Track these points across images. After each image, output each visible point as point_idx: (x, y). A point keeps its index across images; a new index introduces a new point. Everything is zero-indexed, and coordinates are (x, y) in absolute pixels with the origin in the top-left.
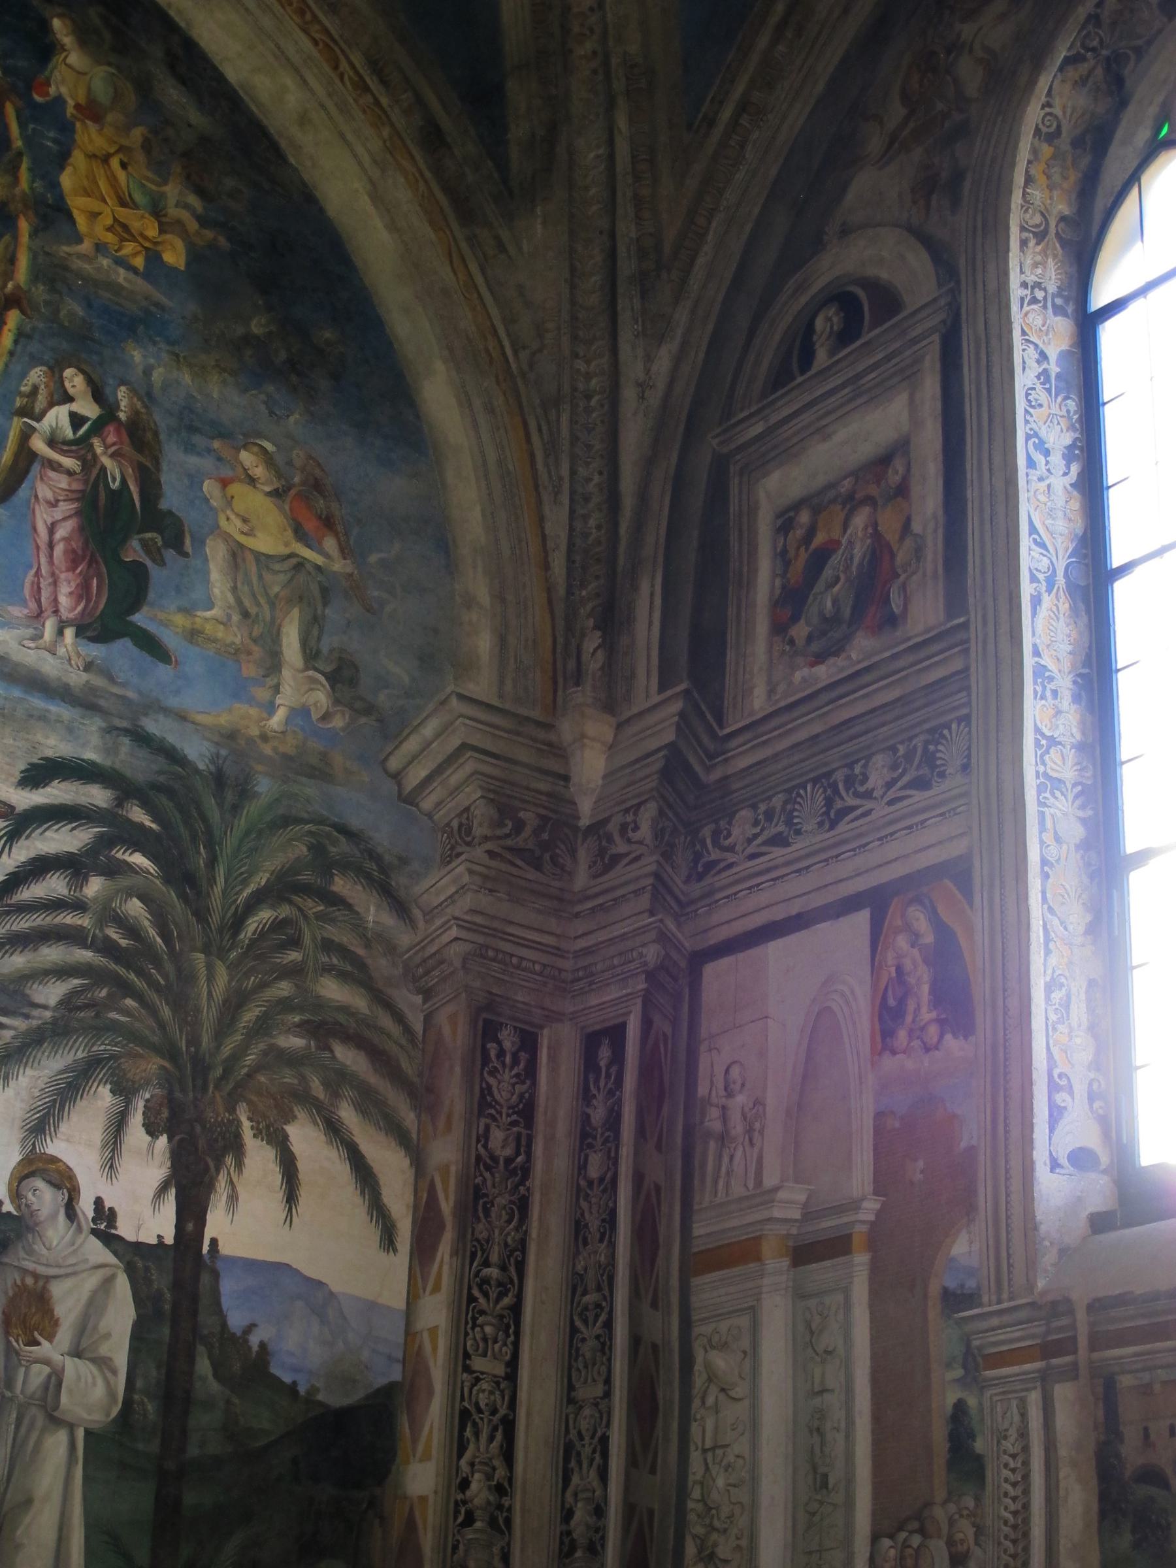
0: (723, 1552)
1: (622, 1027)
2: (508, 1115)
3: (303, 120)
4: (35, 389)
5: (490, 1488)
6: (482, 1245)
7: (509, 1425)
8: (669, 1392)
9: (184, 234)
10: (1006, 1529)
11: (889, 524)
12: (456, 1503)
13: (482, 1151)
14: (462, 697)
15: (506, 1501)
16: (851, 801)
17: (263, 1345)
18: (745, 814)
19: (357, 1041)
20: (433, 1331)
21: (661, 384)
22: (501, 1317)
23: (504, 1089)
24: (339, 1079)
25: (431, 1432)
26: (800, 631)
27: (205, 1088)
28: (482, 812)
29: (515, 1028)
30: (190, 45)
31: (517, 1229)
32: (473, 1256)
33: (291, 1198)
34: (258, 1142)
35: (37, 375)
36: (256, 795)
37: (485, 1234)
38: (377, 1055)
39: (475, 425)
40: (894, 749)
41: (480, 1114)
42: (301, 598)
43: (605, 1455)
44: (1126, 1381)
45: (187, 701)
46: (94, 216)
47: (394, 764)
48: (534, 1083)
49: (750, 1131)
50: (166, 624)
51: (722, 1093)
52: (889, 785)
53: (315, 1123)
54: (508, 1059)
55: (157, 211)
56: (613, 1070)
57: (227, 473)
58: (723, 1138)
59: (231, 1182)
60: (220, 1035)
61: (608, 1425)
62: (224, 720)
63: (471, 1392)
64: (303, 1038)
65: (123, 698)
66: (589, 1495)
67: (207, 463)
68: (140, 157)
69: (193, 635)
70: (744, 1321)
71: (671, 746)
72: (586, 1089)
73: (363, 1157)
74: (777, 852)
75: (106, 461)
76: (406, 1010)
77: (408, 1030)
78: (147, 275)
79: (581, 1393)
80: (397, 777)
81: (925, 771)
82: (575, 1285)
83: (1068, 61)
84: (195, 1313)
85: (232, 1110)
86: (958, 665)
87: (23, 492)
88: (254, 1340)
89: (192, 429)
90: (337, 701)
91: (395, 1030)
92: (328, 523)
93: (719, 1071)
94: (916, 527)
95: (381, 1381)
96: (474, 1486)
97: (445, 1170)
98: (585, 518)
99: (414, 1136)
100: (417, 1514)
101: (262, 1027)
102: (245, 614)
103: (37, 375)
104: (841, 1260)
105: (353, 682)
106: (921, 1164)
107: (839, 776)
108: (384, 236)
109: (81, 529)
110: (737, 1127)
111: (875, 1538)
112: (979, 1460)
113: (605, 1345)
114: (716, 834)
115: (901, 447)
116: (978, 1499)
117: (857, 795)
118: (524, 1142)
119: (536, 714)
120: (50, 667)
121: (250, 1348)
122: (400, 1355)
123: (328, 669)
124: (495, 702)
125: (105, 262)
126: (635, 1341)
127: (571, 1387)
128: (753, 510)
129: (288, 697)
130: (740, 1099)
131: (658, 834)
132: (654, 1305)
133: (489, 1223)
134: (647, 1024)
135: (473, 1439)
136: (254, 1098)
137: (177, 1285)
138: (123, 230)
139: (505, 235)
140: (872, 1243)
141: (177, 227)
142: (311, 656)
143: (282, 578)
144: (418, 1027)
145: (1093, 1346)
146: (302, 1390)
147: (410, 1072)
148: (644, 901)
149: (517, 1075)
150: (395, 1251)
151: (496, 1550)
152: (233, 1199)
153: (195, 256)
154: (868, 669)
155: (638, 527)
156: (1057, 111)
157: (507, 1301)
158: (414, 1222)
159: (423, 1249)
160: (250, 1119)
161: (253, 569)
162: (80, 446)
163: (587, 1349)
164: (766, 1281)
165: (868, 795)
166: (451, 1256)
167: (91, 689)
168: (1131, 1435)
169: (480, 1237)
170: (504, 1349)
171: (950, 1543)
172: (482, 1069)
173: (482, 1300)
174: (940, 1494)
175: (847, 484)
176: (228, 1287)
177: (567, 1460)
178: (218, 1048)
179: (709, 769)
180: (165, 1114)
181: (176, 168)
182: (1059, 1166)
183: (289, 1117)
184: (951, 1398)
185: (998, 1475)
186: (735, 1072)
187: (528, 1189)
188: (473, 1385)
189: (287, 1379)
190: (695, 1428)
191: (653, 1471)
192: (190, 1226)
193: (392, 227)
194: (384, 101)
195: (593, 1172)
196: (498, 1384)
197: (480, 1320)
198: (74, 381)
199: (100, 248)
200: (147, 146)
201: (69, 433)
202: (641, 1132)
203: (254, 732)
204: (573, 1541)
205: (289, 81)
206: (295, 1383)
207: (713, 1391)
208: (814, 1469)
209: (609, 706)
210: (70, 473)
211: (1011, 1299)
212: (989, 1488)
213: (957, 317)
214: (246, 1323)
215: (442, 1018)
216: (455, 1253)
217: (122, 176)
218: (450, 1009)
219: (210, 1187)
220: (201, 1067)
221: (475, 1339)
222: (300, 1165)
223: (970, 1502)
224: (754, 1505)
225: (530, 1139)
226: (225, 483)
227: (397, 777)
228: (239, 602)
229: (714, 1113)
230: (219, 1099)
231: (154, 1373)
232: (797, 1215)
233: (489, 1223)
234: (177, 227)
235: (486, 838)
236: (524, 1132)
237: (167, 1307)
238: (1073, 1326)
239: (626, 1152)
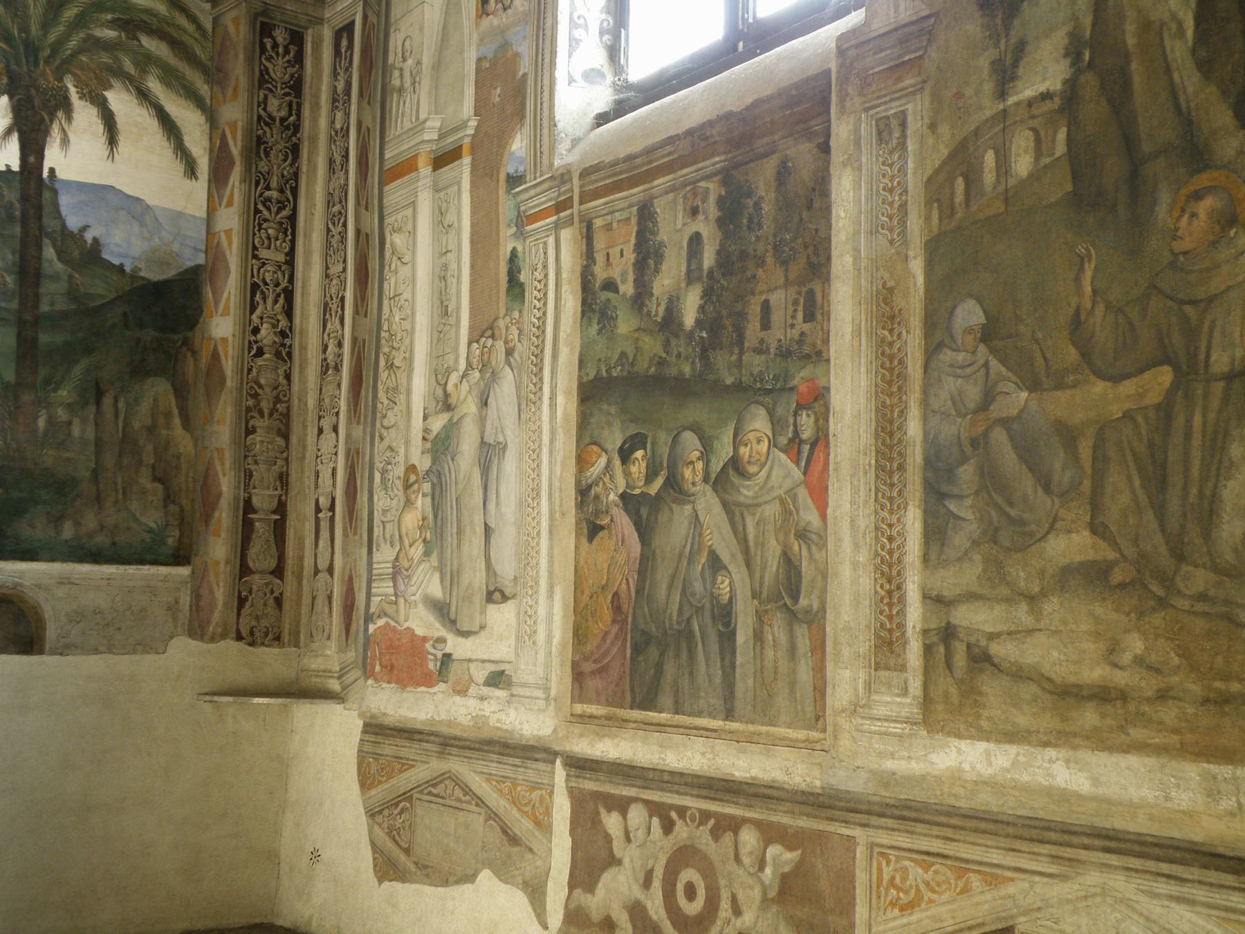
0: (397, 363)
1: (353, 22)
2: (282, 89)
5: (275, 333)
6: (264, 176)
7: (289, 295)
8: (373, 265)
10: (535, 330)
12: (250, 342)
13: (262, 113)
15: (288, 342)
17: (95, 240)
19: (159, 34)
20: (228, 232)
22: (281, 224)
23: (278, 70)
24: (145, 61)
25: (229, 298)
27: (36, 63)
29: (286, 28)
31: (291, 165)
32: (257, 183)
33: (112, 140)
34: (83, 103)
37: (266, 169)
38: (174, 43)
41: (260, 87)
43: (343, 309)
44: (598, 223)
48: (302, 67)
49: (414, 83)
51: (401, 59)
53: (128, 90)
54: (281, 50)
56: (348, 54)
58: (401, 90)
59: (63, 130)
60: (46, 26)
61: (344, 290)
63: (259, 272)
64: (115, 30)
66: (335, 334)
70: (409, 212)
72: (335, 69)
73: (168, 114)
76: (198, 14)
77: (200, 27)
79: (331, 272)
82: (329, 203)
84: (40, 218)
85: (60, 80)
88: (89, 236)
91: (190, 27)
93: (400, 44)
95: (189, 264)
96: (263, 332)
97: (233, 125)
99: (208, 101)
100: (220, 349)
101: (81, 21)
104: (456, 163)
106: (498, 90)
110: (408, 83)
111: (470, 344)
112: (522, 285)
113: (343, 240)
116: (520, 312)
118: (294, 107)
121: (85, 241)
122: (203, 248)
126: (358, 232)
127: (327, 268)
130: (410, 62)
132: (367, 209)
133: (269, 161)
134: (365, 17)
135: (261, 302)
136: (78, 72)
137: (24, 198)
140: (473, 150)
144: (209, 26)
145: (581, 203)
146: (128, 269)
147: (203, 57)
149: (288, 61)
150: (196, 178)
151: (281, 372)
152: (65, 141)
157: (285, 213)
158: (210, 160)
159: (218, 176)
160: (76, 87)
163: (334, 242)
164: (420, 184)
166: (240, 183)
168: (600, 258)
169: (262, 170)
170: (284, 244)
171: (506, 342)
172: (261, 57)
173: (265, 212)
174: (502, 312)
176: (65, 201)
177: (325, 315)
178: (45, 35)
180: (5, 80)
182: (574, 81)
183: (109, 87)
184: (509, 249)
185: (531, 294)
186: (408, 43)
187: (299, 139)
188: (260, 268)
189: (116, 262)
190: (386, 285)
191: (366, 316)
192: (32, 159)
195: (338, 126)
196: (280, 267)
197: (265, 225)
202: (361, 94)
204: (328, 364)
206: (122, 265)
207: (395, 259)
208: (442, 303)
211: (541, 176)
212: (526, 304)
214: (80, 225)
215: (228, 20)
216: (243, 181)
218: (234, 13)
219: (46, 132)
220: (32, 49)
221: (261, 238)
222: (117, 119)
223: (516, 314)
224: (413, 328)
225: (299, 105)
229: (396, 73)
230: (48, 71)
231: (10, 256)
232: (435, 137)
233: (269, 161)
236: (295, 100)
237: (18, 213)
238: (571, 190)
239: (354, 108)
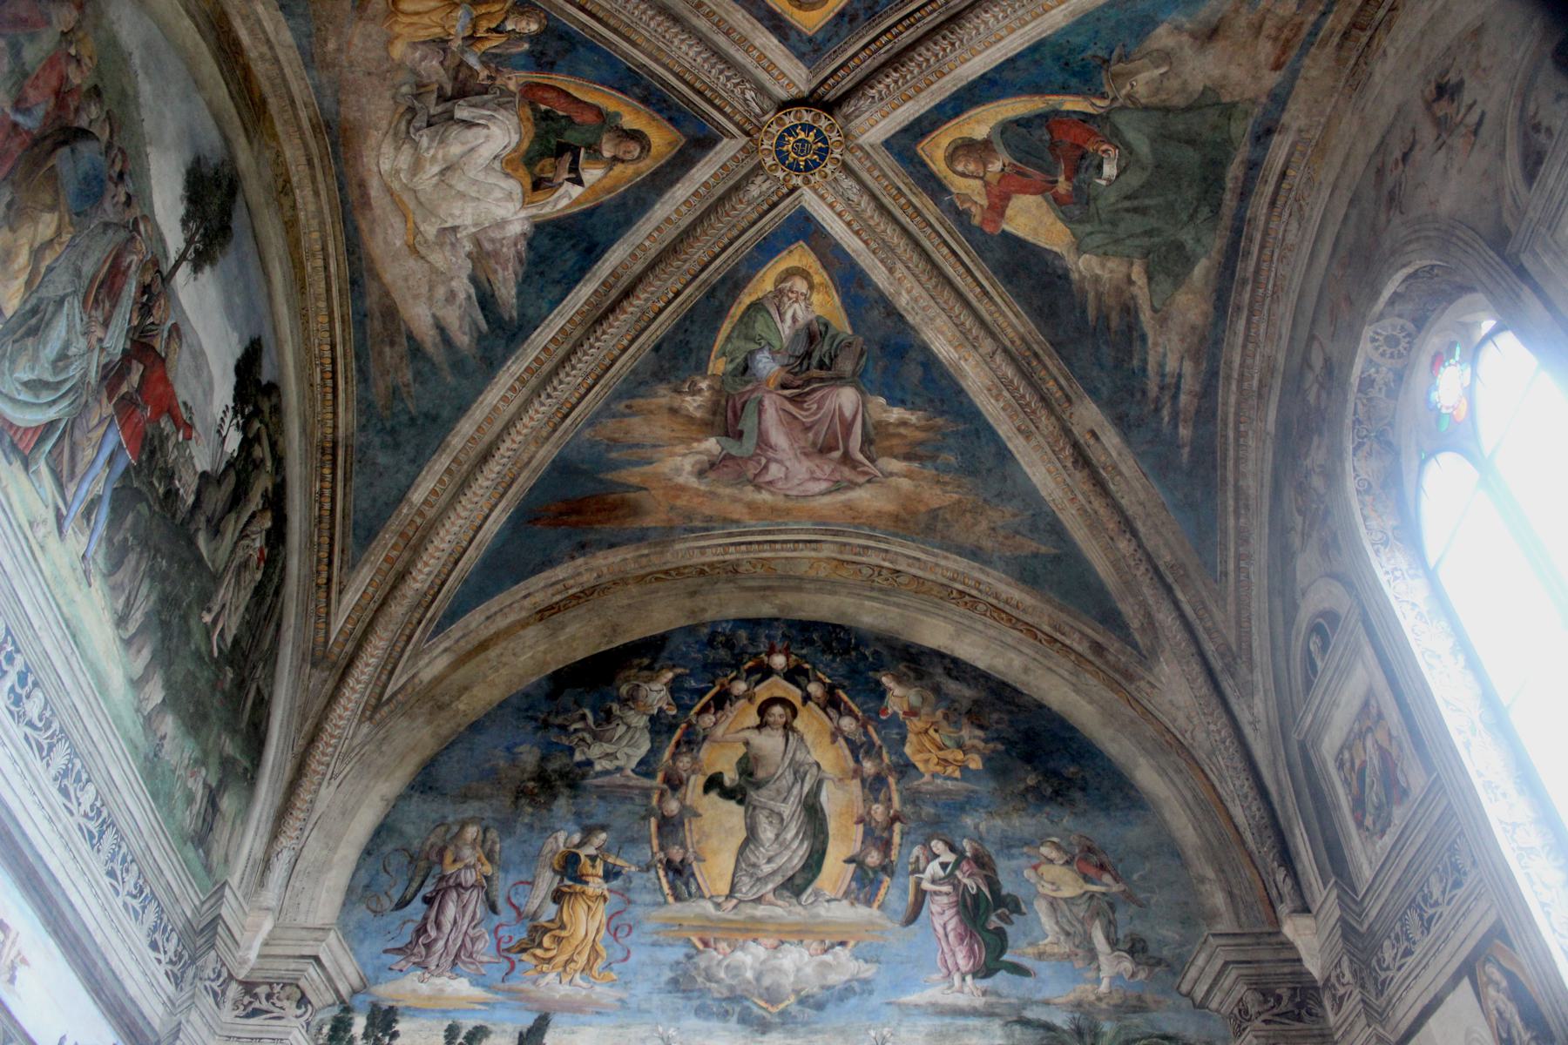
3: (1026, 670)
4: (918, 858)
9: (978, 751)
11: (1381, 735)
14: (1214, 935)
16: (1431, 911)
18: (1387, 943)
21: (1262, 717)
26: (1368, 821)
28: (1252, 1000)
30: (955, 661)
35: (917, 851)
36: (1104, 1034)
39: (1174, 784)
40: (1437, 869)
42: (1097, 914)
45: (1046, 993)
46: (927, 761)
47: (1185, 988)
50: (1024, 955)
52: (1444, 892)
55: (960, 746)
57: (1035, 861)
62: (1072, 997)
65: (1009, 1004)
67: (1023, 861)
68: (944, 723)
69: (1040, 956)
71: (1341, 919)
74: (1410, 960)
75: (966, 881)
78: (964, 779)
80: (1189, 995)
81: (1456, 875)
83: (1355, 450)
86: (1445, 802)
87: (924, 912)
89: (1009, 847)
90: (1138, 964)
92: (1102, 867)
94: (1394, 733)
98: (1249, 807)
102: (1068, 934)
103: (917, 851)
105: (1144, 950)
107: (1419, 899)
108: (1089, 708)
109: (961, 921)
114: (1378, 961)
115: (1370, 693)
117: (1432, 906)
119: (1267, 929)
120: (962, 1000)
123: (1127, 946)
124: (1238, 931)
125: (939, 781)
128: (1324, 763)
129: (1107, 972)
131: (1354, 974)
138: (945, 762)
139: (1152, 679)
141: (974, 748)
142: (1113, 943)
143: (1084, 907)
148: (1363, 1020)
153: (987, 760)
154: (1406, 826)
155: (1282, 799)
156: (1364, 476)
161: (1065, 907)
162: (950, 878)
165: (1436, 904)
167: (991, 1005)
175: (1356, 726)
179: (1361, 924)
181: (965, 720)
193: (1091, 701)
194: (1068, 642)
198: (938, 846)
199: (934, 775)
200: (946, 717)
201: (942, 874)
203: (1092, 998)
205: (1012, 655)
209: (1305, 909)
210: (947, 894)
213: (1363, 607)
217: (936, 736)
226: (1035, 868)
227: (1189, 995)
228: (1062, 929)
234: (974, 748)
235: (1259, 1013)
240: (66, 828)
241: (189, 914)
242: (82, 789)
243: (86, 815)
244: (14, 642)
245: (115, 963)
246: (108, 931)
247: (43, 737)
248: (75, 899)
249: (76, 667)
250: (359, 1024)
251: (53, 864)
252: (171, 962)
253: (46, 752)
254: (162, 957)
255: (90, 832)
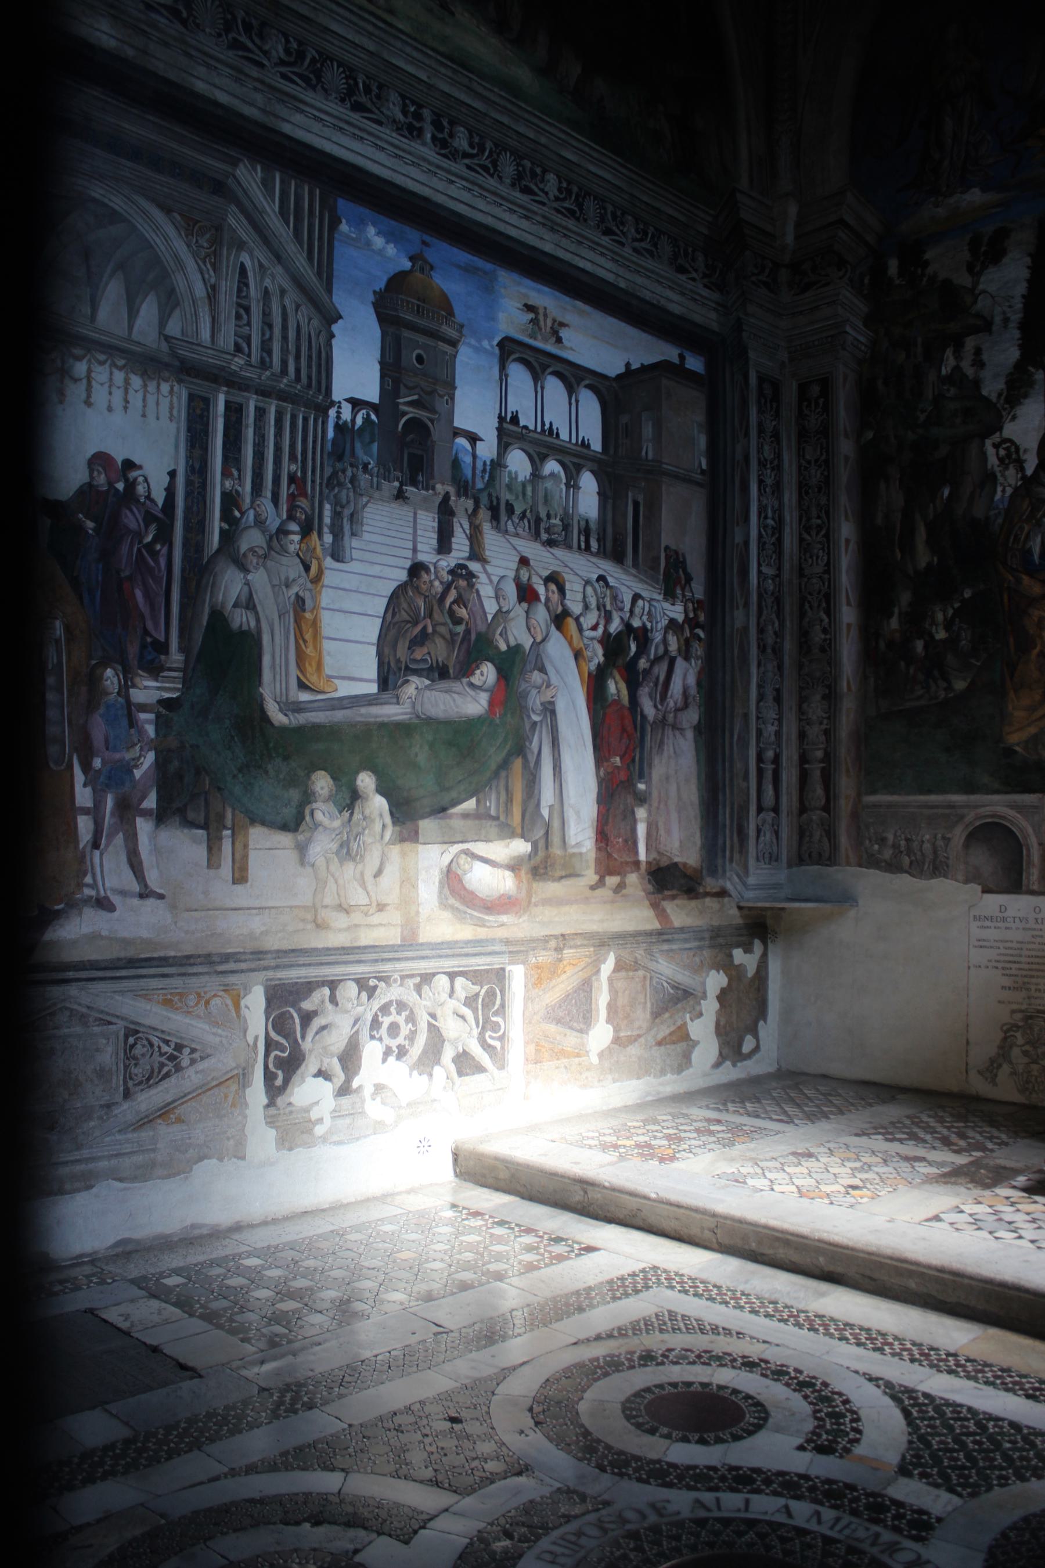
240: (544, 217)
241: (705, 231)
242: (542, 181)
243: (557, 199)
244: (413, 103)
245: (647, 295)
246: (628, 275)
247: (484, 160)
248: (581, 264)
249: (480, 90)
250: (893, 267)
251: (548, 248)
252: (705, 276)
253: (493, 169)
254: (694, 275)
255: (568, 210)
